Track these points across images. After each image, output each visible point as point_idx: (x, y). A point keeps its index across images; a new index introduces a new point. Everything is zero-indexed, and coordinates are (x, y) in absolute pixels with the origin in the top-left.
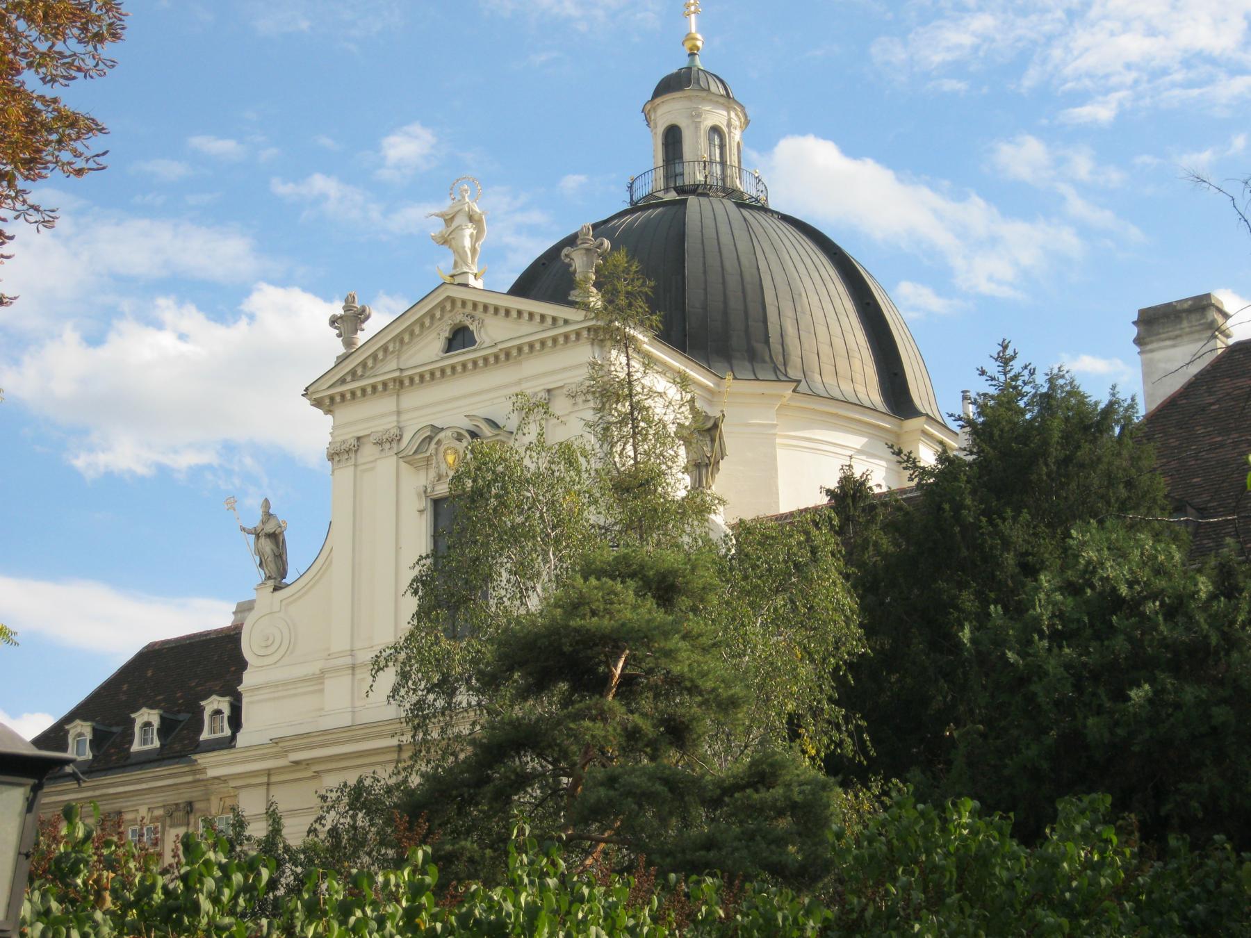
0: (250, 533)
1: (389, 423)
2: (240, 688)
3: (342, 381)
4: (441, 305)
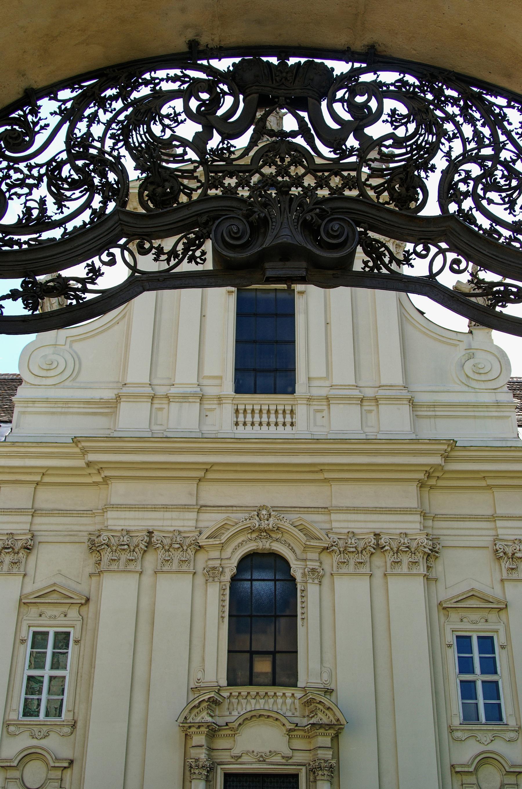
2: (14, 398)
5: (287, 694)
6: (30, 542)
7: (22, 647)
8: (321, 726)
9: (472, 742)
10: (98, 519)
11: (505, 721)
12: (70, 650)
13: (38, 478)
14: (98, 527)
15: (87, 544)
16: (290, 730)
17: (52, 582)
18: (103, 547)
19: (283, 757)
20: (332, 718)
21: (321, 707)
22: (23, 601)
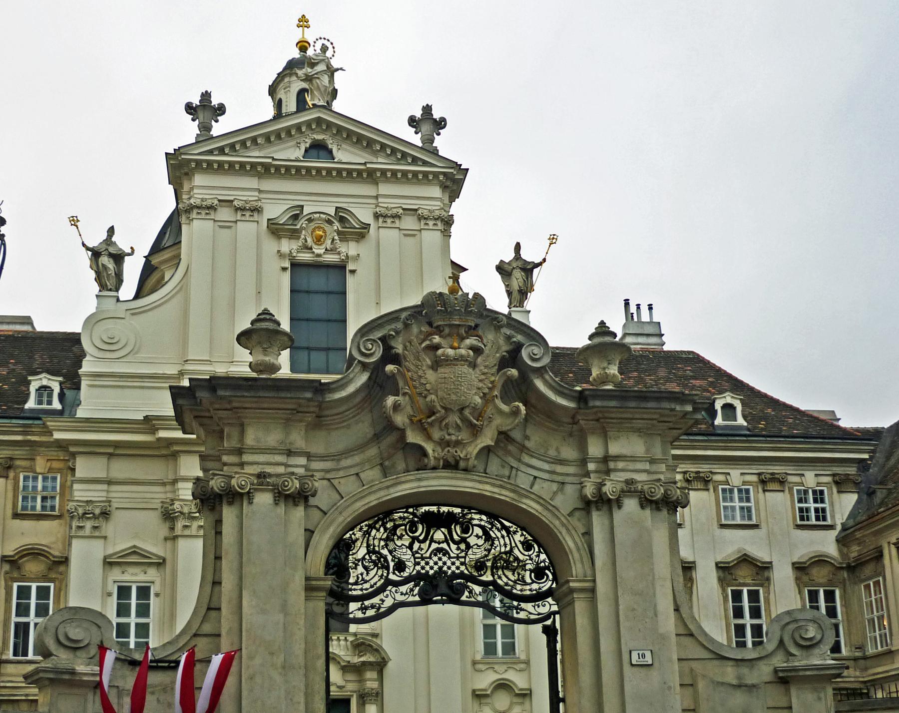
0: (88, 249)
1: (252, 196)
3: (210, 152)
4: (308, 123)
5: (340, 638)
6: (108, 508)
7: (109, 599)
8: (370, 663)
9: (490, 672)
10: (168, 488)
11: (517, 656)
12: (152, 602)
13: (111, 450)
14: (170, 495)
15: (160, 510)
16: (345, 666)
17: (133, 545)
18: (177, 514)
19: (338, 687)
20: (378, 656)
21: (370, 648)
22: (108, 560)
